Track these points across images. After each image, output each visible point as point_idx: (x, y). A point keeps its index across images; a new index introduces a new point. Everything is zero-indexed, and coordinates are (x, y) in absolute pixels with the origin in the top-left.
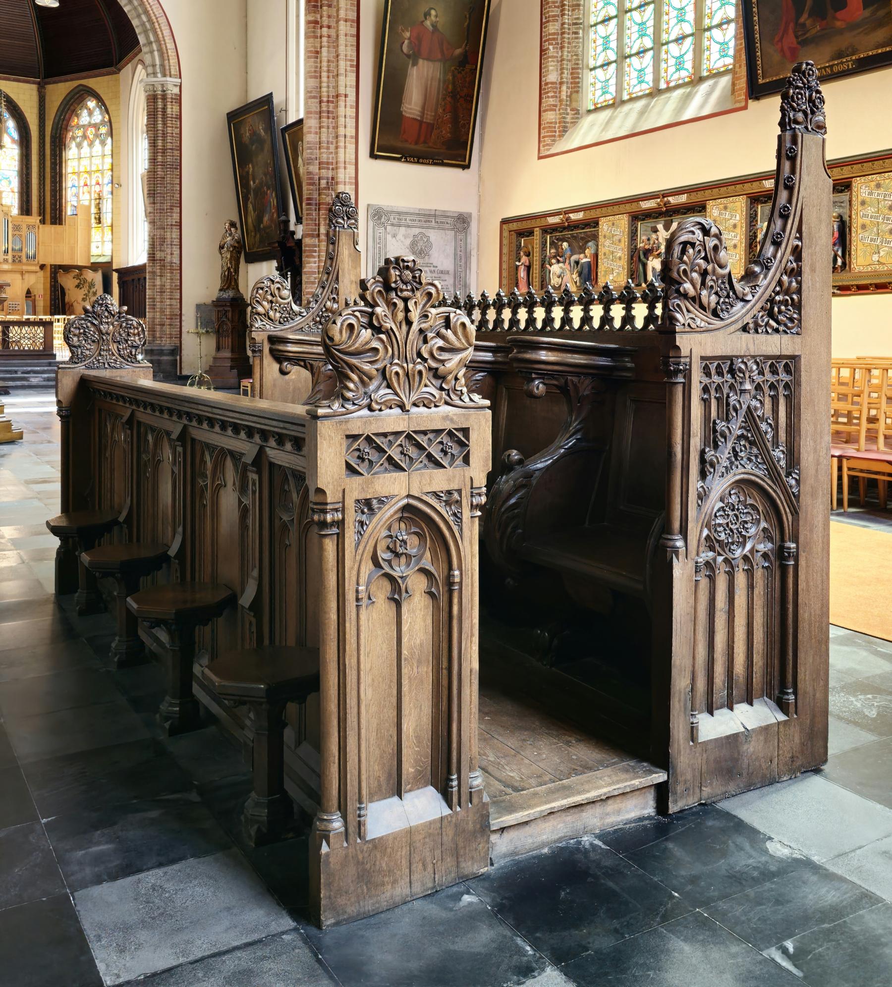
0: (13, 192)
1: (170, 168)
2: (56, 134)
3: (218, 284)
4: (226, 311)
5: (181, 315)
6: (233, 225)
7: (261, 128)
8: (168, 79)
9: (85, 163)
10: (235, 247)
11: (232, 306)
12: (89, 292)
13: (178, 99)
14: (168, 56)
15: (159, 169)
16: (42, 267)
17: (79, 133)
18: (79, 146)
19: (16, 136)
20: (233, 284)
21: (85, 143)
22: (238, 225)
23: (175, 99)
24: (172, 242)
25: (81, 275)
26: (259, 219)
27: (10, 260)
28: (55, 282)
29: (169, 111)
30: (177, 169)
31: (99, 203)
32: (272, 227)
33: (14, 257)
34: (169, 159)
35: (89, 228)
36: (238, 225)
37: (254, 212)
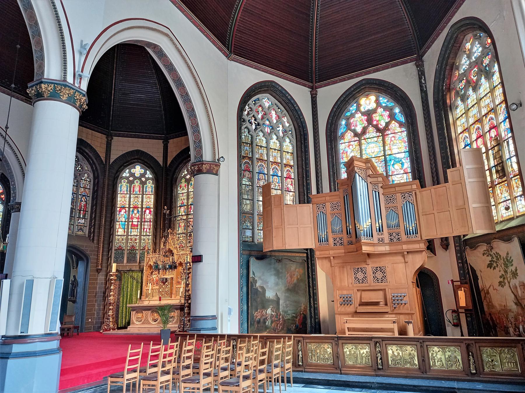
2: (438, 97)
12: (506, 272)
19: (402, 119)
27: (387, 240)
28: (462, 263)
33: (391, 235)
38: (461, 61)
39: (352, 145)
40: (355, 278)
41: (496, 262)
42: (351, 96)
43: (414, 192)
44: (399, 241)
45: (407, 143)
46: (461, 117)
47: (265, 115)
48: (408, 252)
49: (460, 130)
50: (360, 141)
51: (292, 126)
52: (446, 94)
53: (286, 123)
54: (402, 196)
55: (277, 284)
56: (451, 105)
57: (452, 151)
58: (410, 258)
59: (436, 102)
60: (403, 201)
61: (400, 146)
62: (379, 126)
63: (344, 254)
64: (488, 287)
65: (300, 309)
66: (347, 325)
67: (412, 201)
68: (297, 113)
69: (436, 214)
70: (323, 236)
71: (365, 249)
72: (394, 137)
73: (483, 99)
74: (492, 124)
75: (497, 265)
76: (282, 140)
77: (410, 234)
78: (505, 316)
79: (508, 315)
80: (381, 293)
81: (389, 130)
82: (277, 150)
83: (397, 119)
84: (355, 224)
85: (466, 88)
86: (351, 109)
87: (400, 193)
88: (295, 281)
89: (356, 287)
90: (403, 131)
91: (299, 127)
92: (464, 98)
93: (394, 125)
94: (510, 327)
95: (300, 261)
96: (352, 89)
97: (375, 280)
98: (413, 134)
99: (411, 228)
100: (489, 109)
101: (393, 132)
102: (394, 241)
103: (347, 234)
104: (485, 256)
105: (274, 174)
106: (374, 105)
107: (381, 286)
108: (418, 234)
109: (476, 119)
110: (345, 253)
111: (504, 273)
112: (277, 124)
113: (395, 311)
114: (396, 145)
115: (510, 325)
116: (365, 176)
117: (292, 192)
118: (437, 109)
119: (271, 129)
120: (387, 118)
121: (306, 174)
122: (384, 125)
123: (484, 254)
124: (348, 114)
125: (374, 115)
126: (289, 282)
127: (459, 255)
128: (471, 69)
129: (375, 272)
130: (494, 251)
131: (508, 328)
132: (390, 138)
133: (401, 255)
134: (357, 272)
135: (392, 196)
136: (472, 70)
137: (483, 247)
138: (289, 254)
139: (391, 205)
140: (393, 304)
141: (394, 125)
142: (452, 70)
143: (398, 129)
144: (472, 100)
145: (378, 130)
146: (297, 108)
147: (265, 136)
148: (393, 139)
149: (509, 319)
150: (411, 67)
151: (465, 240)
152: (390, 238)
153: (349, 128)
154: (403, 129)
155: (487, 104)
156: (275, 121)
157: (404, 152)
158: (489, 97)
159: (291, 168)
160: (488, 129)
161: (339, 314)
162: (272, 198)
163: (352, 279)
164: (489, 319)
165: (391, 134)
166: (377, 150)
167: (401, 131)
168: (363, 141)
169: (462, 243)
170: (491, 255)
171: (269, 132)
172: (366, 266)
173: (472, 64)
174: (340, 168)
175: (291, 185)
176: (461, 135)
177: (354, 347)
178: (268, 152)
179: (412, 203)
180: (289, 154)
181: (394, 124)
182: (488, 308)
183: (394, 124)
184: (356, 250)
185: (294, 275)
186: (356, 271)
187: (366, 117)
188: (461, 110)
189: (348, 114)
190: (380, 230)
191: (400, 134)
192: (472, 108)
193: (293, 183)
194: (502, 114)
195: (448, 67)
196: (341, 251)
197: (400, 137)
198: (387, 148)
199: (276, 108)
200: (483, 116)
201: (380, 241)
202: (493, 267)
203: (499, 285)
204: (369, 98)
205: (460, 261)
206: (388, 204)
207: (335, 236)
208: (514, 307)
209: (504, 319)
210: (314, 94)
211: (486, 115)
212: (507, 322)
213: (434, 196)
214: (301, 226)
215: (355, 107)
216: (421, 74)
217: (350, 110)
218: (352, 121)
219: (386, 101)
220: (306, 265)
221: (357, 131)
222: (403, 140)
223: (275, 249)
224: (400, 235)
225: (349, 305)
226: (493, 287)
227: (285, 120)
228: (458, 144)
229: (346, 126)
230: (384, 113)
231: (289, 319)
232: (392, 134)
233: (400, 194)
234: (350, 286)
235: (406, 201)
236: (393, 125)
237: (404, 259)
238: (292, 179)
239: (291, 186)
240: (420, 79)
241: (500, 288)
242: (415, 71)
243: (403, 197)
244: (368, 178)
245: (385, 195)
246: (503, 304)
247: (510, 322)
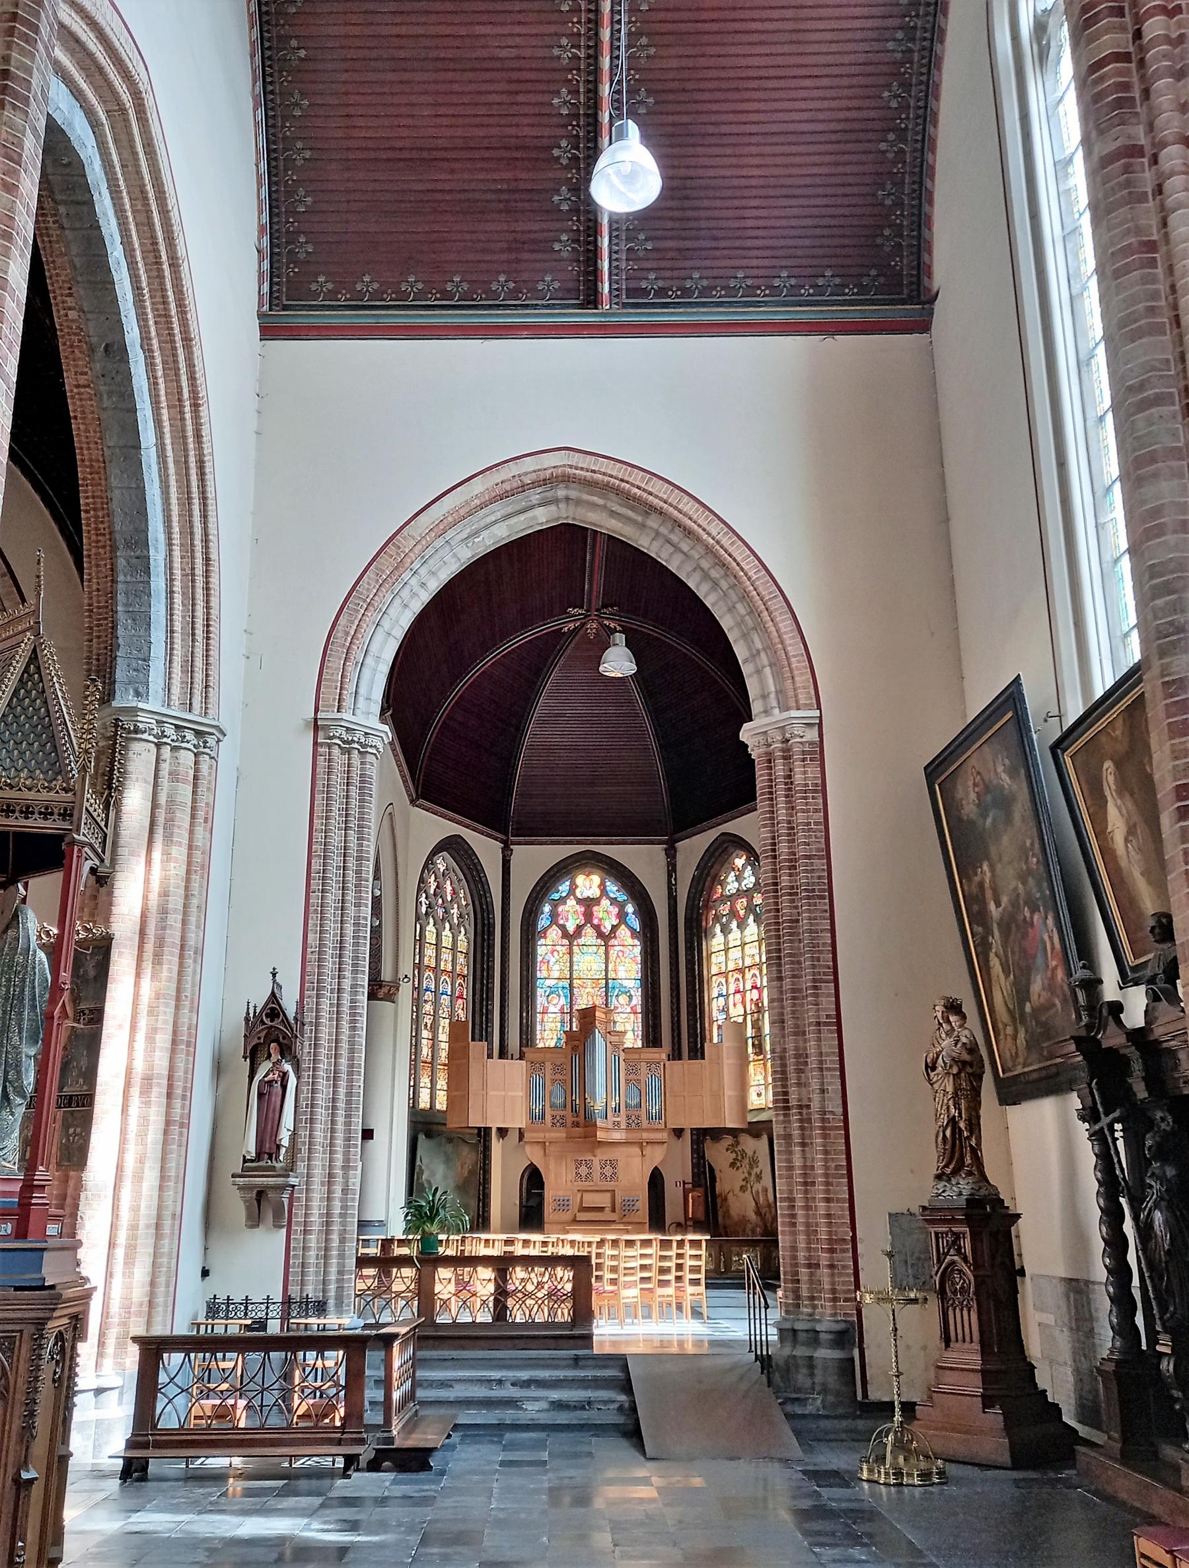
0: (635, 1013)
1: (808, 898)
3: (932, 1161)
4: (957, 1236)
5: (854, 1239)
6: (953, 1007)
7: (1000, 769)
8: (794, 713)
9: (735, 954)
10: (964, 1063)
11: (969, 1221)
12: (750, 1174)
13: (817, 753)
14: (791, 670)
15: (785, 902)
16: (678, 1133)
17: (724, 909)
18: (725, 930)
20: (968, 1160)
21: (734, 924)
22: (969, 1008)
23: (809, 753)
24: (821, 1062)
25: (738, 1143)
26: (1021, 992)
27: (623, 1126)
29: (798, 778)
30: (823, 898)
31: (758, 1019)
32: (1054, 1005)
33: (629, 1117)
34: (802, 878)
35: (743, 1063)
36: (969, 1008)
37: (1007, 976)
50: (571, 946)
58: (648, 1150)
71: (600, 1135)
80: (608, 1195)
81: (615, 937)
88: (466, 1174)
92: (725, 930)
93: (623, 932)
106: (595, 892)
107: (610, 1185)
124: (556, 896)
125: (595, 908)
130: (740, 1148)
137: (728, 1140)
139: (632, 1076)
141: (623, 932)
143: (630, 941)
145: (600, 935)
150: (658, 850)
156: (449, 898)
163: (571, 1175)
166: (595, 967)
168: (575, 949)
189: (556, 896)
190: (617, 1110)
196: (560, 1134)
198: (611, 967)
207: (554, 1113)
208: (752, 1216)
216: (672, 869)
219: (615, 888)
240: (670, 876)
241: (741, 1194)
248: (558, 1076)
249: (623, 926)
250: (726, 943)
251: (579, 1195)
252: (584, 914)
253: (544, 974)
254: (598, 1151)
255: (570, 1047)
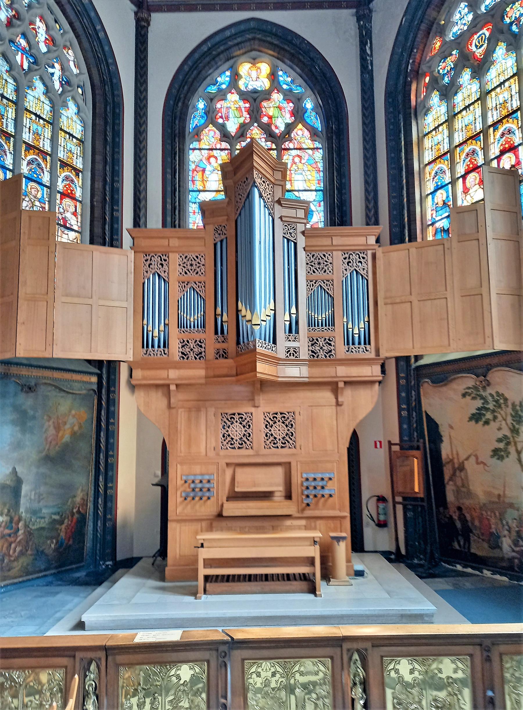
19: (318, 125)
27: (304, 354)
33: (313, 342)
38: (450, 14)
39: (216, 158)
40: (224, 436)
41: (493, 411)
42: (222, 48)
43: (370, 253)
44: (330, 357)
45: (322, 174)
46: (434, 132)
47: (18, 19)
48: (346, 383)
49: (428, 157)
51: (86, 77)
52: (411, 82)
53: (72, 64)
54: (345, 259)
55: (18, 446)
56: (418, 107)
57: (411, 196)
59: (389, 95)
60: (346, 270)
61: (310, 177)
62: (273, 128)
63: (203, 381)
64: (463, 457)
65: (73, 503)
66: (204, 554)
67: (365, 271)
68: (102, 47)
69: (415, 303)
70: (156, 333)
72: (299, 156)
73: (493, 93)
74: (507, 142)
75: (495, 418)
76: (58, 101)
77: (353, 344)
78: (497, 514)
79: (505, 512)
82: (44, 120)
83: (308, 120)
84: (238, 311)
85: (458, 68)
86: (219, 79)
87: (341, 250)
89: (225, 456)
90: (317, 148)
91: (103, 82)
94: (505, 536)
95: (84, 392)
96: (228, 33)
97: (268, 442)
98: (339, 155)
99: (356, 331)
100: (504, 113)
101: (299, 147)
102: (320, 357)
103: (216, 333)
104: (468, 398)
105: (29, 176)
106: (264, 84)
108: (369, 344)
109: (470, 134)
110: (206, 377)
111: (508, 434)
112: (51, 55)
113: (308, 513)
114: (302, 174)
115: (506, 533)
116: (270, 199)
117: (75, 231)
118: (391, 110)
119: (33, 63)
120: (288, 115)
121: (112, 197)
122: (282, 128)
123: (464, 395)
125: (265, 104)
126: (49, 440)
127: (403, 394)
128: (475, 29)
129: (271, 423)
131: (499, 537)
132: (291, 158)
133: (330, 387)
134: (229, 423)
135: (324, 256)
136: (476, 33)
138: (57, 375)
139: (320, 275)
140: (304, 497)
142: (429, 33)
143: (308, 143)
144: (466, 95)
146: (101, 35)
147: (13, 73)
148: (297, 160)
149: (504, 522)
151: (418, 368)
152: (310, 348)
153: (212, 119)
154: (317, 145)
155: (501, 102)
156: (43, 49)
157: (316, 191)
158: (510, 87)
159: (77, 175)
160: (497, 153)
161: (178, 521)
162: (24, 218)
164: (455, 517)
165: (294, 149)
167: (312, 146)
169: (412, 372)
170: (482, 398)
171: (26, 66)
172: (253, 410)
173: (478, 20)
174: (187, 201)
175: (75, 214)
176: (428, 168)
177: (279, 669)
178: (19, 115)
179: (362, 276)
180: (74, 140)
181: (301, 129)
182: (457, 498)
183: (301, 129)
184: (234, 372)
185: (65, 423)
186: (227, 421)
187: (247, 105)
188: (435, 117)
189: (213, 89)
191: (310, 152)
192: (464, 112)
193: (79, 210)
194: (496, 143)
195: (423, 27)
197: (310, 158)
199: (50, 19)
200: (490, 126)
201: (290, 354)
202: (484, 419)
203: (492, 456)
204: (258, 65)
205: (404, 406)
206: (314, 272)
209: (493, 521)
210: (143, 19)
211: (495, 125)
212: (500, 526)
213: (414, 263)
214: (101, 302)
215: (228, 79)
217: (217, 82)
218: (218, 106)
219: (289, 79)
220: (96, 402)
221: (229, 129)
222: (315, 166)
223: (21, 352)
224: (332, 343)
225: (204, 498)
226: (477, 458)
227: (70, 55)
228: (422, 183)
229: (205, 113)
230: (285, 104)
231: (42, 529)
232: (297, 149)
233: (340, 253)
234: (212, 454)
235: (352, 269)
236: (300, 132)
237: (337, 398)
238: (77, 200)
239: (74, 218)
240: (363, 44)
242: (353, 27)
243: (347, 260)
244: (277, 206)
245: (308, 251)
246: (496, 492)
247: (507, 527)
248: (192, 276)
249: (300, 126)
250: (450, 108)
251: (229, 473)
252: (249, 111)
253: (199, 186)
254: (262, 399)
255: (211, 228)
